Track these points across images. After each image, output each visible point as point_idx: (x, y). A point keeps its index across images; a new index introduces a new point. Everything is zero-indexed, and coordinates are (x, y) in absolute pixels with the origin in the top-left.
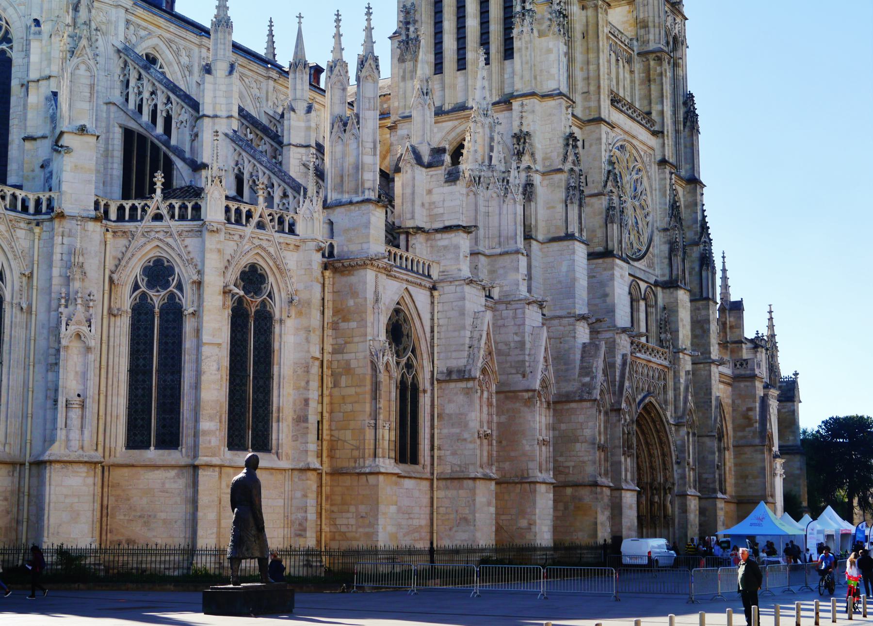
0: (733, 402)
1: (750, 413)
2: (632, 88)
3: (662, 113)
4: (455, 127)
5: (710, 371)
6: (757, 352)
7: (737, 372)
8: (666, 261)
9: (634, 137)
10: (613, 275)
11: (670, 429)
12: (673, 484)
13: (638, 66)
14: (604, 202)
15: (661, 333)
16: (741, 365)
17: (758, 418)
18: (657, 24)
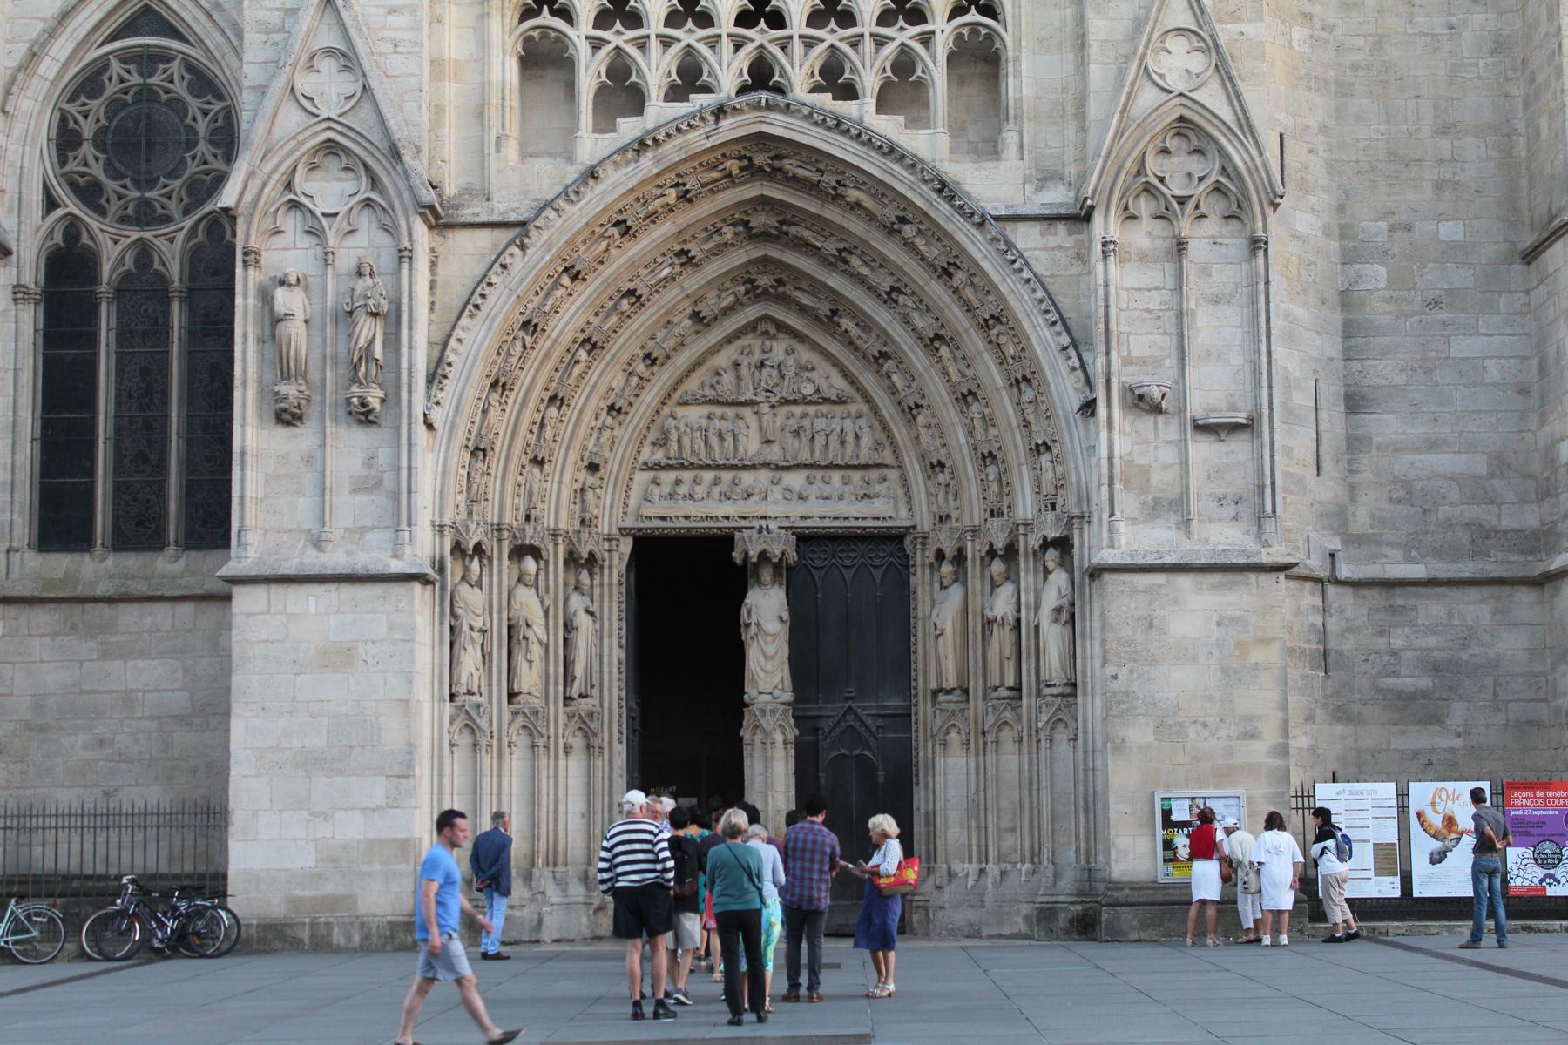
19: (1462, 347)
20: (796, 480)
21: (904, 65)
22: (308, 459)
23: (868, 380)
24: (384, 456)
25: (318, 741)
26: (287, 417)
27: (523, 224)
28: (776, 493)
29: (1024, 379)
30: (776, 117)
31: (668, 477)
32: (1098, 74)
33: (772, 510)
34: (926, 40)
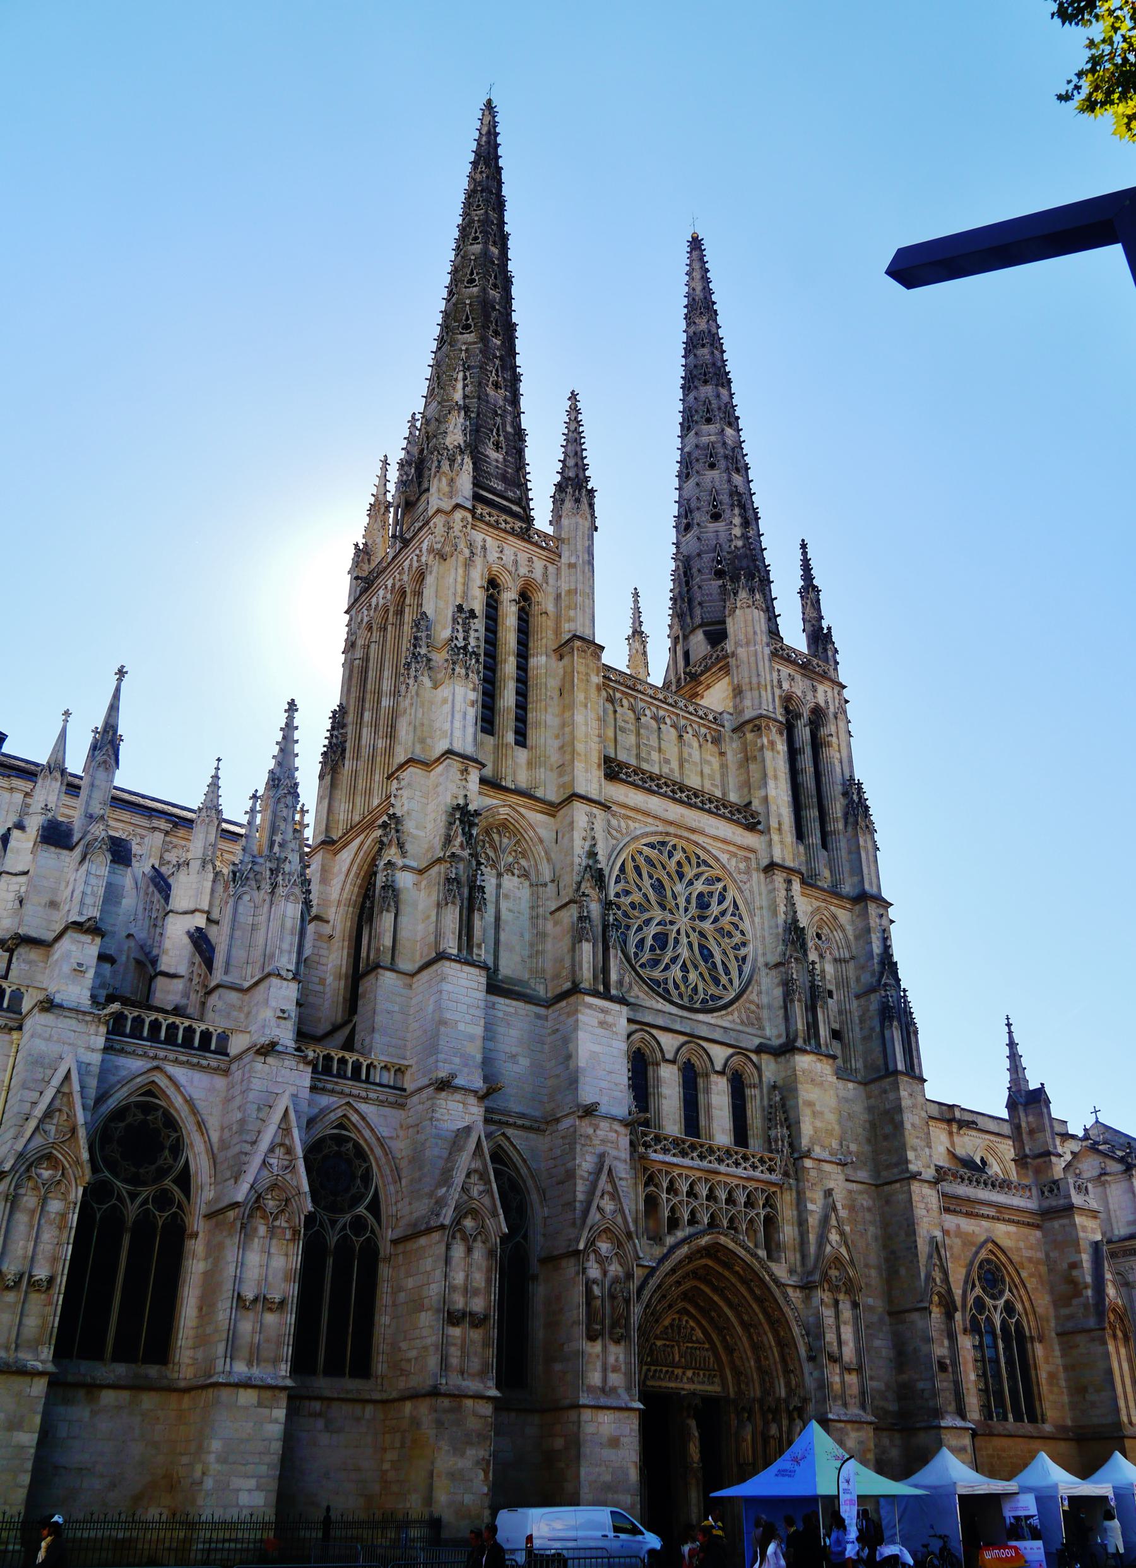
0: (1047, 1255)
1: (1075, 1273)
2: (724, 775)
3: (765, 800)
4: (362, 843)
5: (910, 1193)
6: (1131, 1176)
7: (1046, 1204)
8: (781, 1012)
9: (693, 831)
10: (577, 1021)
11: (785, 1295)
12: (805, 1400)
13: (732, 748)
14: (573, 910)
15: (769, 1128)
16: (1051, 1191)
17: (1089, 1279)
18: (755, 686)
19: (877, 1343)
20: (689, 1373)
21: (751, 1221)
22: (598, 1356)
23: (714, 1336)
24: (622, 1357)
25: (608, 1478)
26: (592, 1338)
27: (653, 1268)
28: (685, 1380)
29: (785, 1344)
30: (722, 1237)
31: (653, 1368)
32: (812, 1237)
33: (687, 1386)
34: (758, 1214)
